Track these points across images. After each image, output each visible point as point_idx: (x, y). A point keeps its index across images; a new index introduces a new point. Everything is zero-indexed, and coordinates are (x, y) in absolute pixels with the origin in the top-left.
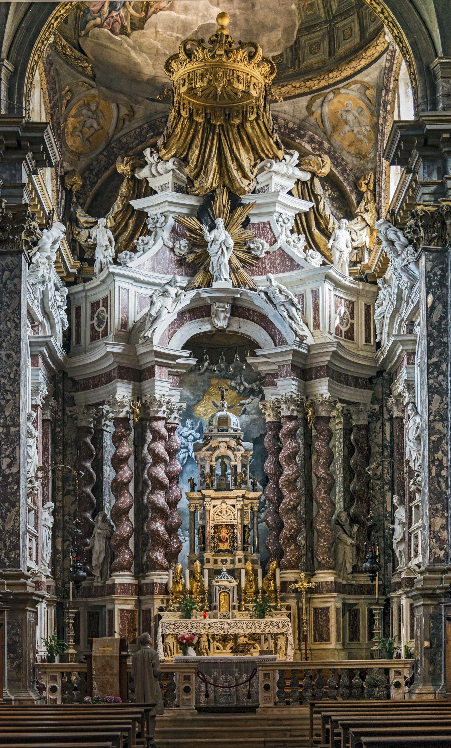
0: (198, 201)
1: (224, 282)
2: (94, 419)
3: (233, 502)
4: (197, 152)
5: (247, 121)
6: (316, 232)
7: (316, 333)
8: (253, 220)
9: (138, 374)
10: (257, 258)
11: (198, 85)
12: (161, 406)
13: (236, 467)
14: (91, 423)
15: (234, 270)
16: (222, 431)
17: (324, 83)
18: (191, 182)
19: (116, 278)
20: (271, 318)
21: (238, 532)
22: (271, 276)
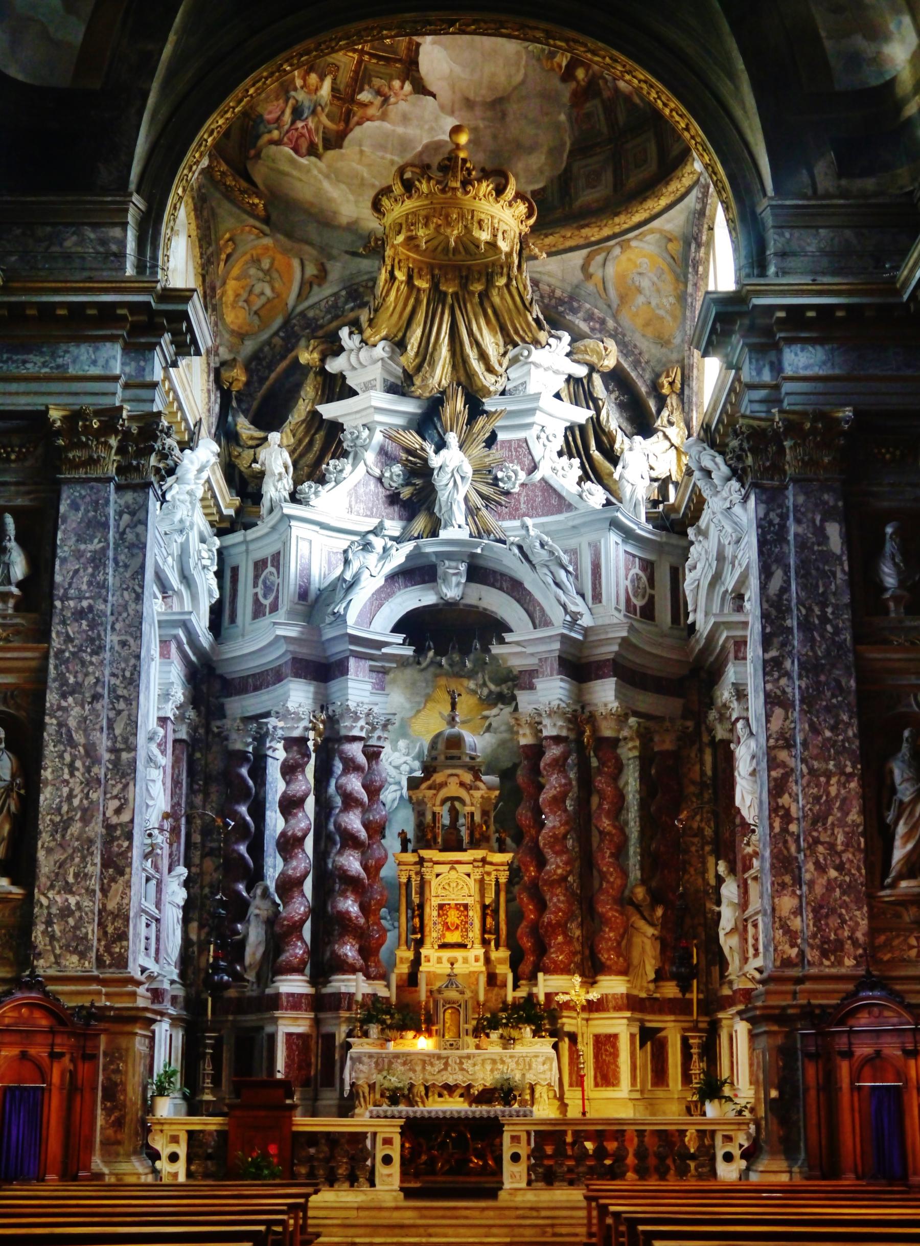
0: (420, 407)
1: (456, 530)
2: (254, 739)
3: (468, 868)
4: (418, 332)
6: (596, 455)
7: (597, 608)
8: (501, 436)
9: (323, 670)
10: (507, 493)
11: (421, 232)
12: (357, 718)
13: (472, 814)
14: (248, 745)
15: (472, 511)
16: (452, 758)
18: (408, 377)
19: (293, 523)
20: (527, 585)
21: (475, 915)
22: (529, 521)
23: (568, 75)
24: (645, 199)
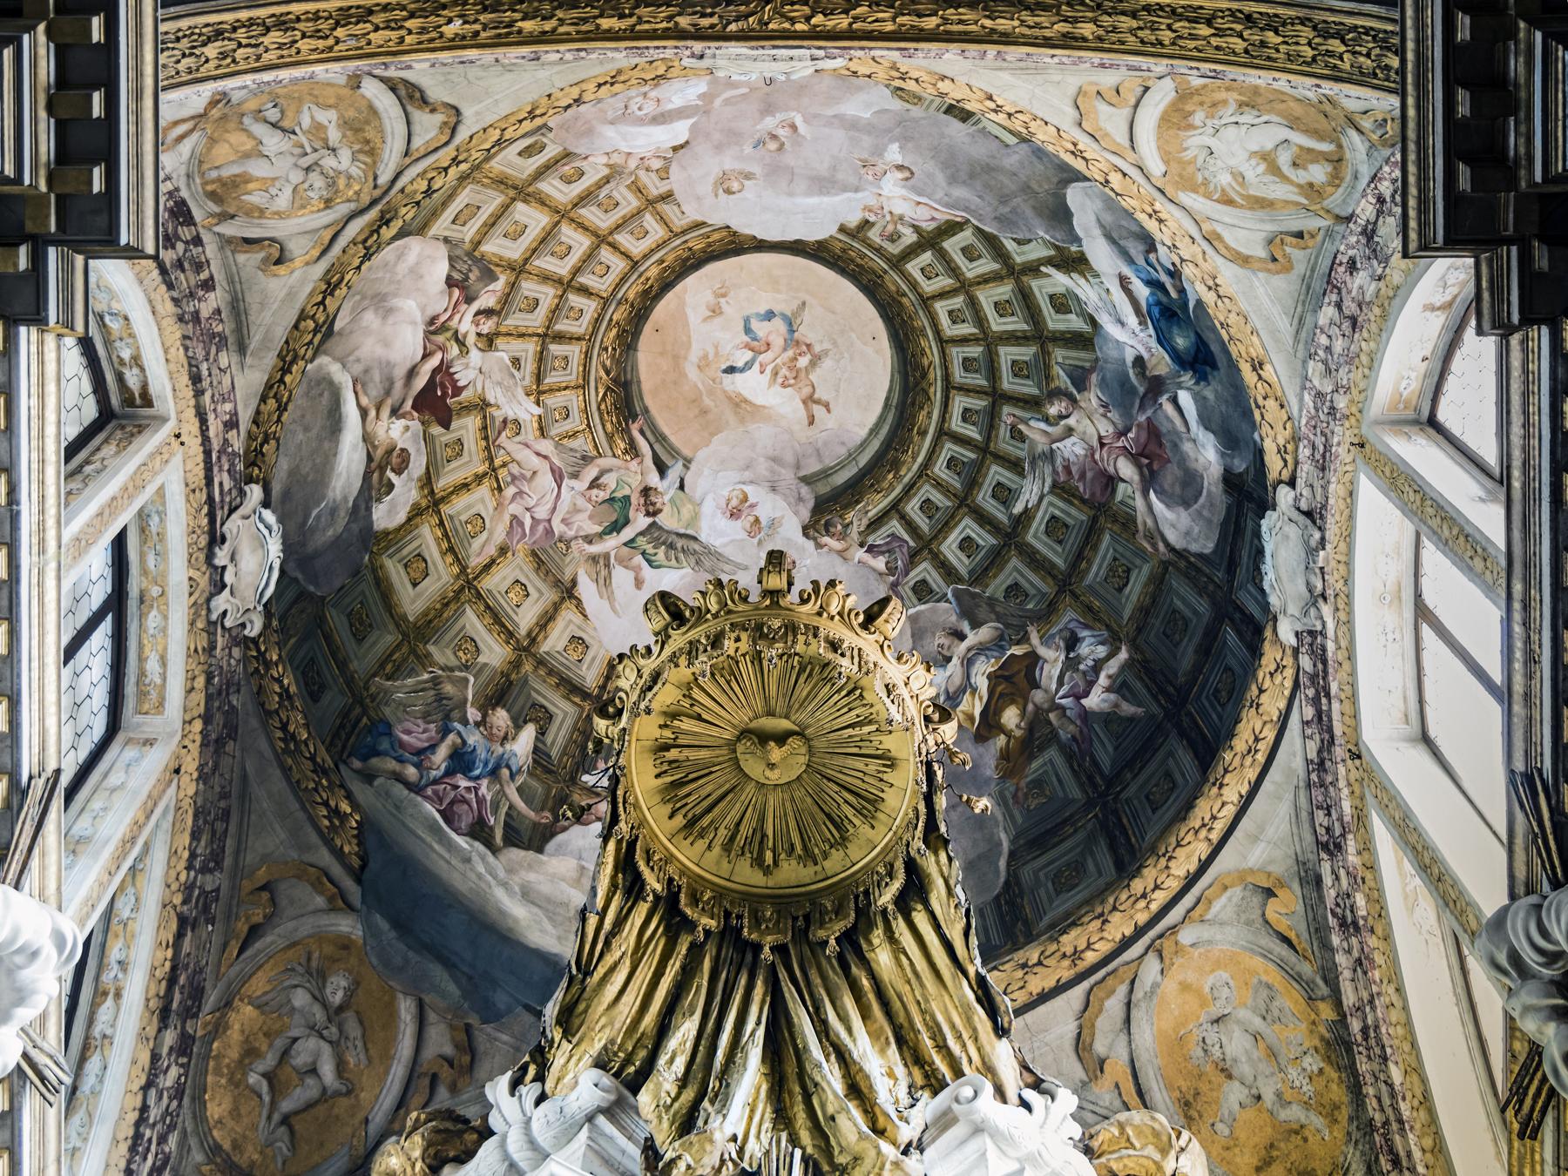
5: (871, 926)
24: (1189, 806)
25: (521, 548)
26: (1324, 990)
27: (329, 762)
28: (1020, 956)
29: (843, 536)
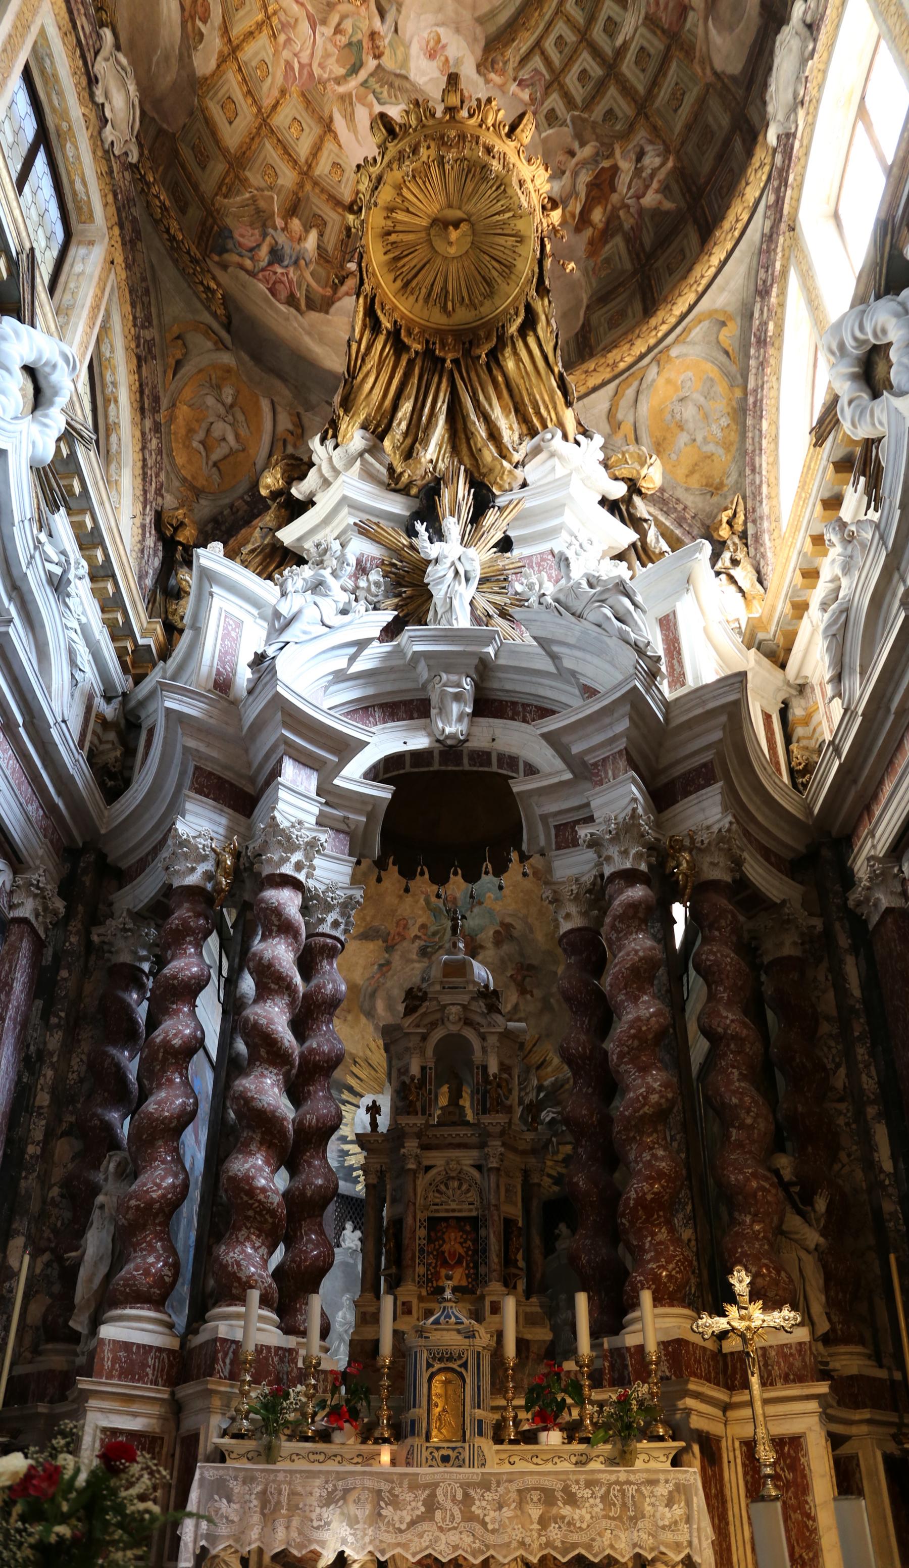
17: (640, 347)
23: (584, 220)
24: (690, 270)
25: (294, 89)
26: (740, 380)
27: (198, 256)
28: (584, 367)
29: (502, 73)
